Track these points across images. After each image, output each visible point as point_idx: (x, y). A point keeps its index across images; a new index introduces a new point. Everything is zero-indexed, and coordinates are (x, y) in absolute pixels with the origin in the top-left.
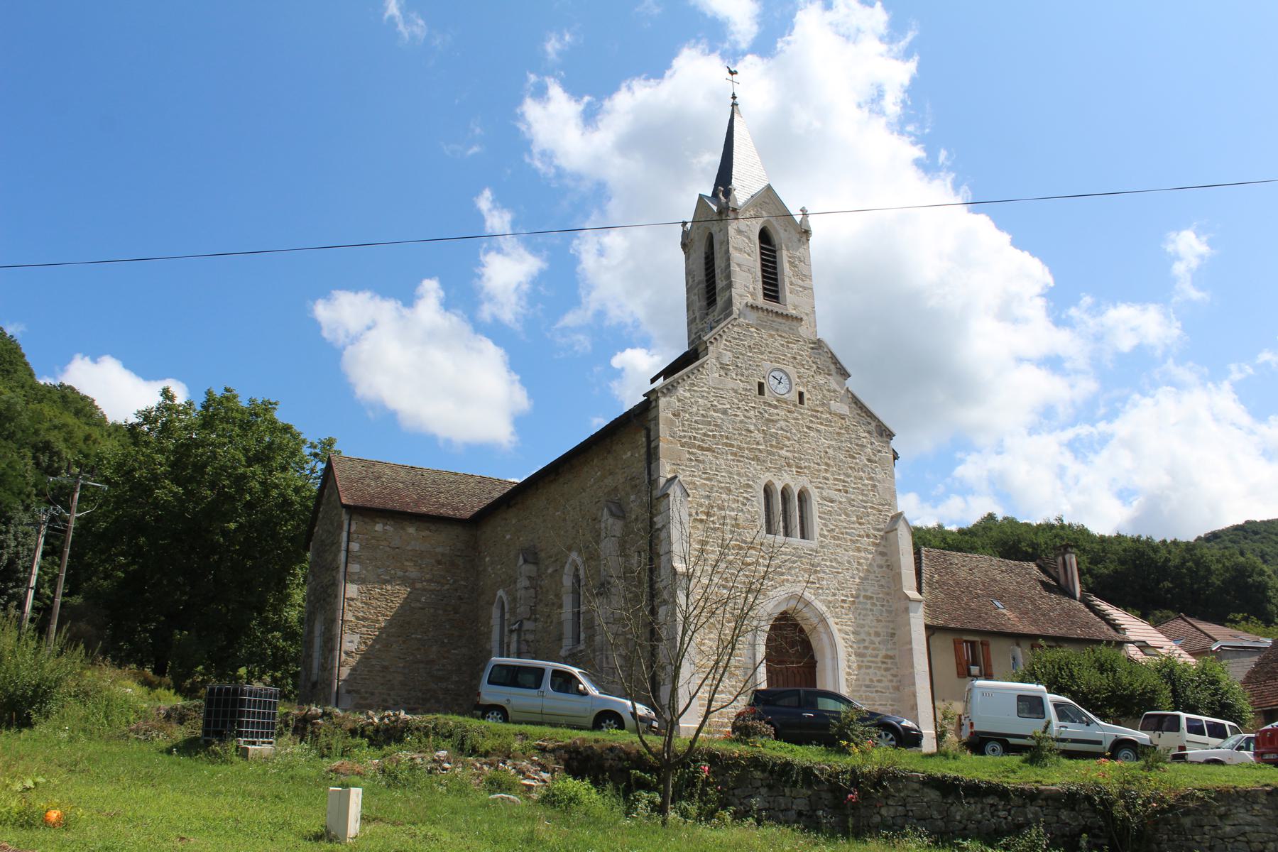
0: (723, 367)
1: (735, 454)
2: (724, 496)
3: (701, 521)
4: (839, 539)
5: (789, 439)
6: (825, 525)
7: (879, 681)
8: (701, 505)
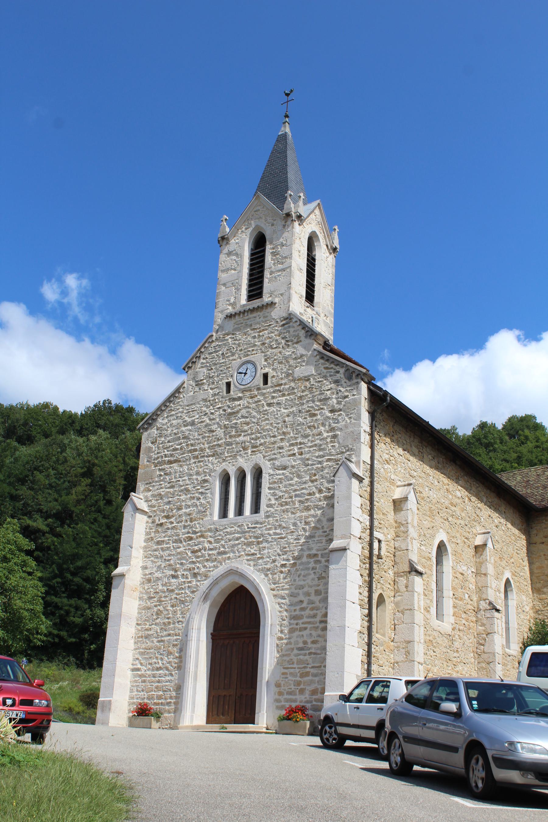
0: (199, 384)
1: (197, 457)
2: (183, 497)
3: (161, 525)
4: (287, 503)
5: (247, 424)
6: (274, 495)
7: (314, 642)
8: (163, 511)
